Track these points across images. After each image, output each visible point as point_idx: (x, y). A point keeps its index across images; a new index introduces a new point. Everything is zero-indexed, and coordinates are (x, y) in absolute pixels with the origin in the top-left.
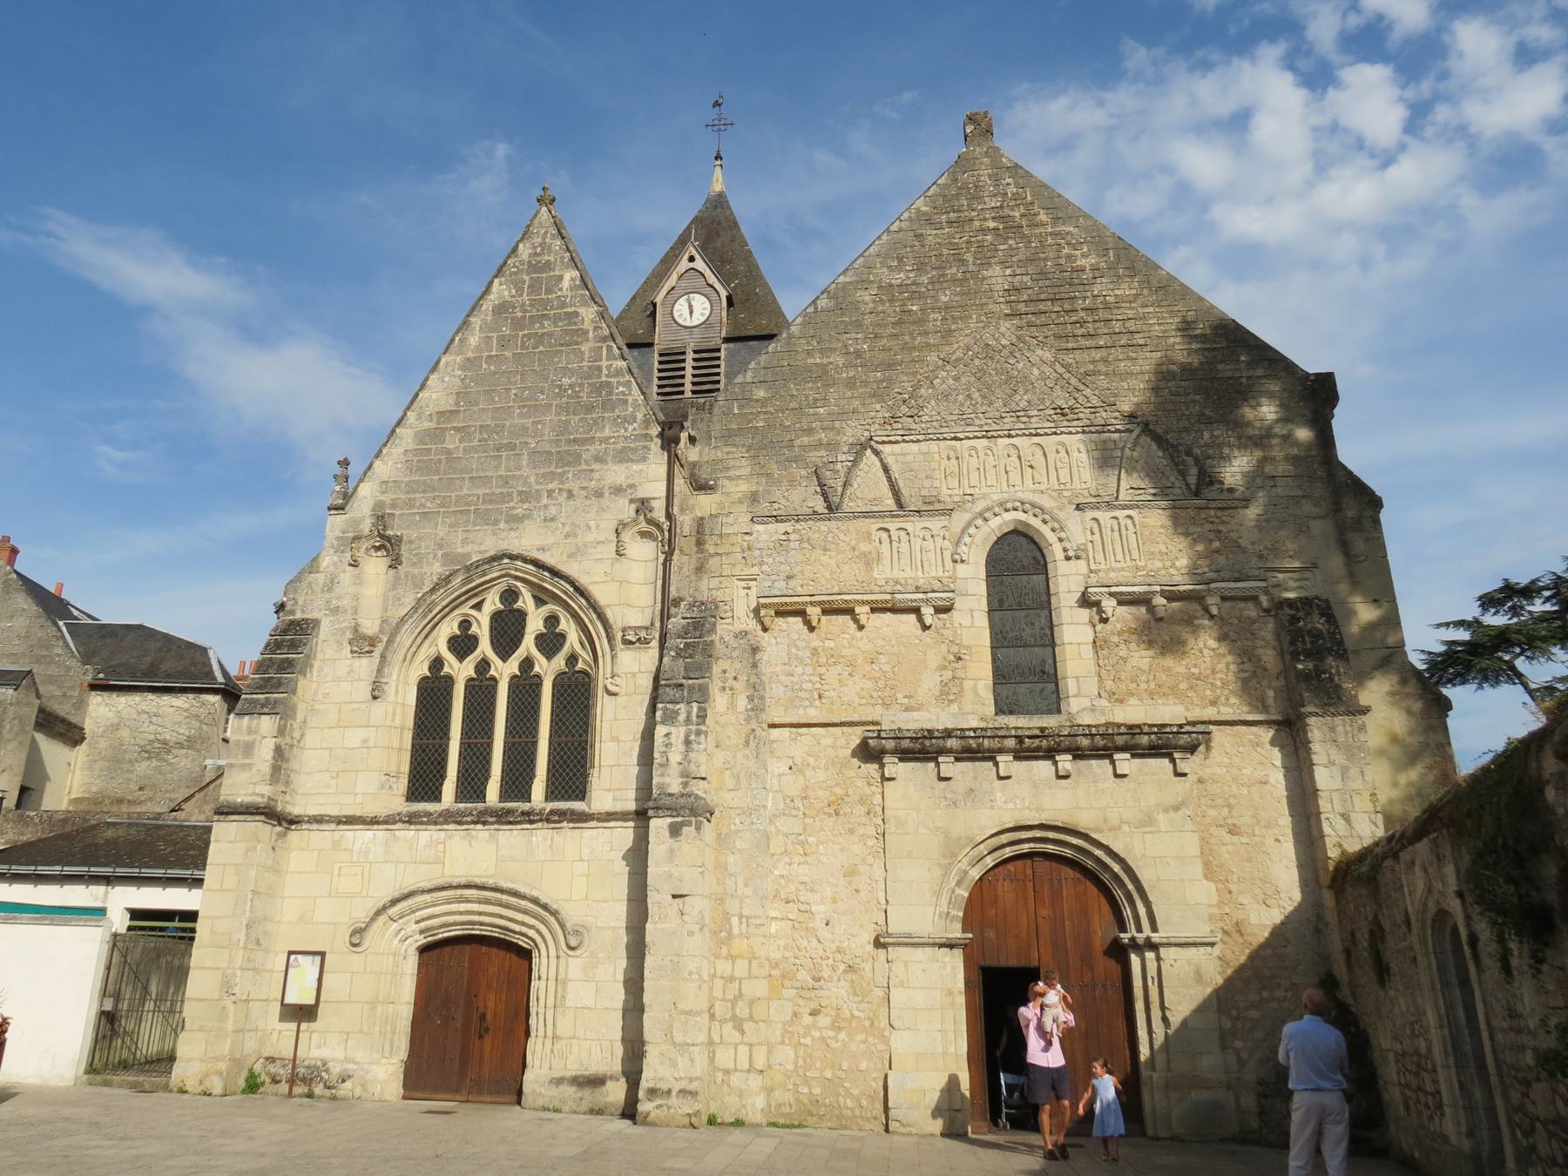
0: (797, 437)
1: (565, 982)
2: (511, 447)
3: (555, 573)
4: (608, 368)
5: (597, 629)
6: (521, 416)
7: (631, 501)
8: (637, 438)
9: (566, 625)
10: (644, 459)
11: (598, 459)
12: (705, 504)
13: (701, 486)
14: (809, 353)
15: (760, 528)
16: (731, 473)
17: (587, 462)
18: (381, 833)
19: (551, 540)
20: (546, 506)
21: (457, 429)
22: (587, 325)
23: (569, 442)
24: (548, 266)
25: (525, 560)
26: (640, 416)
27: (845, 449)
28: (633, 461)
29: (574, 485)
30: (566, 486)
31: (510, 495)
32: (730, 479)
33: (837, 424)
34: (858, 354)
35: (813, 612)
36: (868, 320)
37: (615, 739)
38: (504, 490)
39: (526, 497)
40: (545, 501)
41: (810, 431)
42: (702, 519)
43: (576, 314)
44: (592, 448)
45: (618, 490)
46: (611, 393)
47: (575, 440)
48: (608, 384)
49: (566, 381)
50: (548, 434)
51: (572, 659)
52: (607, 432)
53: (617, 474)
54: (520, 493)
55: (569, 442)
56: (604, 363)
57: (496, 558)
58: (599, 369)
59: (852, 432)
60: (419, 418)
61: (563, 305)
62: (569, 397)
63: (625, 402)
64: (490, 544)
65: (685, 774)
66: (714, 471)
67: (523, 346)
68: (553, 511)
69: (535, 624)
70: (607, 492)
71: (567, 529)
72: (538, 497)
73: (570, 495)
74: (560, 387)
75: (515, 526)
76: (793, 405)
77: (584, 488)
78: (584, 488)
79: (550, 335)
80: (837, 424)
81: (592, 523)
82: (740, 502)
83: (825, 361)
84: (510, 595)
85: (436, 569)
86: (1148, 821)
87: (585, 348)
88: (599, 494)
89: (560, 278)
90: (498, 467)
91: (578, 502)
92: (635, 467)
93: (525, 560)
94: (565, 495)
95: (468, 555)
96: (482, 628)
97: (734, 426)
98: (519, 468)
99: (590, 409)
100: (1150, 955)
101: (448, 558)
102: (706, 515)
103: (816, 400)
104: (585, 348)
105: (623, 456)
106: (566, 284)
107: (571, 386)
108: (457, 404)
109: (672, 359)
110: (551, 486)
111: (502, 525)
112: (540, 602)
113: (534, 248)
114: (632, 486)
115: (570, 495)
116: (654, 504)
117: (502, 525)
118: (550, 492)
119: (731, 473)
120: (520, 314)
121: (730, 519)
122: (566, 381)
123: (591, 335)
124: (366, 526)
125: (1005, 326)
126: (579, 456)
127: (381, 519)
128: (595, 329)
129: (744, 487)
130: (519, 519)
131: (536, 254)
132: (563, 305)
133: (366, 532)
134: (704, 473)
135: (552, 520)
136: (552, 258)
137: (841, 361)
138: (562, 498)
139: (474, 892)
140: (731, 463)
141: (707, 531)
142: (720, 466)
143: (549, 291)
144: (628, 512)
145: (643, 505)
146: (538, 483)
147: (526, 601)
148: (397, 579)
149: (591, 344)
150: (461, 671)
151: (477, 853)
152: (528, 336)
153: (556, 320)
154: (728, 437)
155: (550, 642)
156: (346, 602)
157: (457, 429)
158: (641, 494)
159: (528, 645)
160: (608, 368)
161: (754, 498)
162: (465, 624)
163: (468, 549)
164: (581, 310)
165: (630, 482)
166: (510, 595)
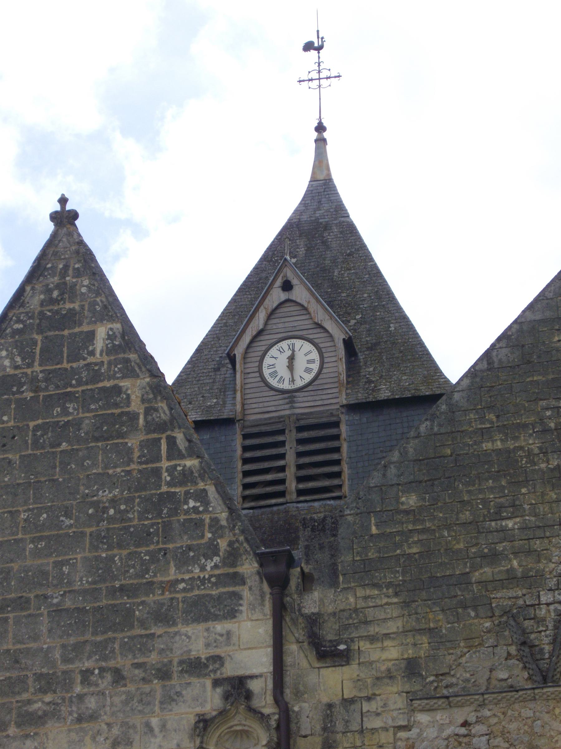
0: (474, 568)
2: (22, 603)
4: (171, 470)
6: (36, 553)
7: (216, 683)
8: (222, 580)
10: (232, 614)
11: (163, 616)
12: (333, 682)
13: (329, 654)
14: (485, 434)
15: (423, 718)
16: (373, 630)
17: (143, 624)
20: (81, 697)
22: (136, 406)
23: (112, 592)
24: (72, 318)
26: (223, 544)
27: (552, 583)
28: (216, 618)
29: (123, 662)
30: (112, 663)
31: (22, 681)
32: (373, 639)
33: (537, 544)
38: (14, 674)
39: (47, 683)
40: (78, 689)
41: (493, 557)
42: (330, 706)
43: (117, 390)
44: (151, 599)
45: (195, 667)
46: (175, 512)
47: (122, 589)
48: (171, 496)
49: (105, 495)
50: (82, 580)
52: (172, 573)
53: (195, 639)
54: (39, 677)
55: (112, 592)
56: (165, 464)
58: (157, 472)
61: (96, 377)
62: (111, 520)
63: (199, 524)
66: (346, 627)
67: (36, 444)
68: (92, 703)
70: (176, 668)
71: (116, 731)
72: (67, 685)
73: (118, 677)
74: (95, 505)
75: (32, 731)
76: (466, 516)
77: (138, 666)
78: (138, 666)
79: (78, 424)
80: (537, 544)
81: (155, 722)
82: (390, 676)
83: (511, 444)
88: (164, 674)
89: (91, 336)
91: (131, 688)
92: (219, 627)
94: (109, 677)
97: (372, 554)
98: (35, 638)
99: (143, 537)
102: (336, 700)
103: (500, 507)
104: (133, 442)
105: (200, 611)
106: (99, 343)
107: (114, 502)
109: (262, 443)
110: (88, 664)
111: (12, 730)
113: (48, 291)
114: (218, 659)
115: (118, 677)
116: (255, 686)
117: (12, 730)
118: (86, 674)
119: (373, 630)
120: (29, 395)
121: (373, 706)
122: (105, 495)
123: (141, 421)
126: (130, 612)
128: (147, 411)
129: (391, 653)
130: (39, 720)
131: (53, 301)
132: (96, 377)
134: (329, 632)
135: (93, 717)
136: (76, 306)
137: (533, 444)
138: (105, 683)
140: (371, 614)
141: (340, 726)
142: (358, 618)
143: (74, 357)
144: (212, 700)
145: (237, 689)
146: (66, 660)
149: (142, 437)
152: (43, 427)
153: (85, 400)
154: (365, 572)
158: (230, 670)
160: (171, 470)
161: (412, 668)
164: (125, 384)
165: (213, 651)
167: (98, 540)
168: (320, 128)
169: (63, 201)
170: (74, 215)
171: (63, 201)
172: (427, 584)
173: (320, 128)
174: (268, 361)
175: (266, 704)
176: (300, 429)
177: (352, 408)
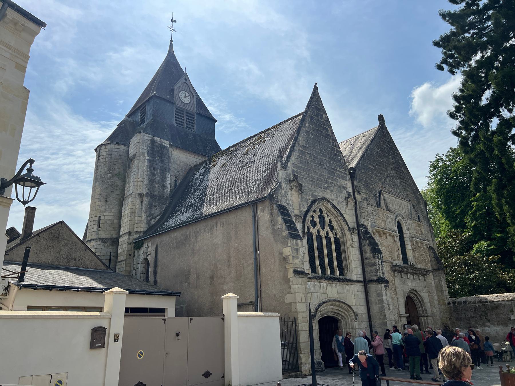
1: (355, 329)
3: (335, 208)
5: (346, 227)
6: (321, 156)
9: (335, 224)
11: (339, 176)
13: (359, 193)
18: (312, 283)
19: (333, 197)
21: (308, 153)
24: (318, 110)
25: (329, 201)
34: (376, 168)
35: (381, 232)
36: (376, 160)
37: (354, 260)
39: (326, 182)
51: (336, 234)
53: (343, 182)
57: (324, 199)
59: (378, 189)
60: (298, 145)
64: (320, 194)
65: (383, 273)
69: (327, 222)
73: (335, 186)
84: (321, 211)
85: (310, 199)
86: (423, 290)
87: (331, 141)
89: (322, 115)
90: (319, 169)
93: (329, 201)
95: (316, 196)
96: (317, 219)
100: (425, 318)
101: (312, 195)
108: (306, 145)
112: (328, 215)
124: (292, 177)
125: (394, 171)
127: (295, 177)
133: (292, 179)
139: (334, 303)
147: (324, 214)
148: (301, 197)
150: (314, 231)
151: (333, 291)
155: (331, 227)
156: (290, 202)
157: (308, 153)
159: (327, 228)
162: (313, 217)
163: (316, 194)
166: (321, 211)
167: (329, 158)
168: (171, 41)
169: (316, 84)
170: (317, 88)
171: (316, 84)
172: (367, 187)
173: (171, 41)
174: (180, 94)
175: (352, 197)
176: (187, 113)
177: (197, 113)
